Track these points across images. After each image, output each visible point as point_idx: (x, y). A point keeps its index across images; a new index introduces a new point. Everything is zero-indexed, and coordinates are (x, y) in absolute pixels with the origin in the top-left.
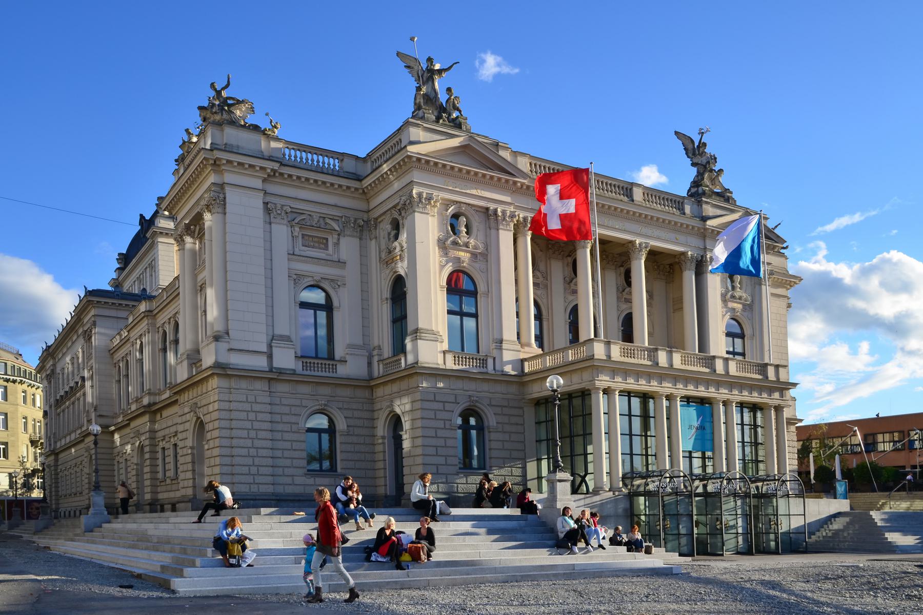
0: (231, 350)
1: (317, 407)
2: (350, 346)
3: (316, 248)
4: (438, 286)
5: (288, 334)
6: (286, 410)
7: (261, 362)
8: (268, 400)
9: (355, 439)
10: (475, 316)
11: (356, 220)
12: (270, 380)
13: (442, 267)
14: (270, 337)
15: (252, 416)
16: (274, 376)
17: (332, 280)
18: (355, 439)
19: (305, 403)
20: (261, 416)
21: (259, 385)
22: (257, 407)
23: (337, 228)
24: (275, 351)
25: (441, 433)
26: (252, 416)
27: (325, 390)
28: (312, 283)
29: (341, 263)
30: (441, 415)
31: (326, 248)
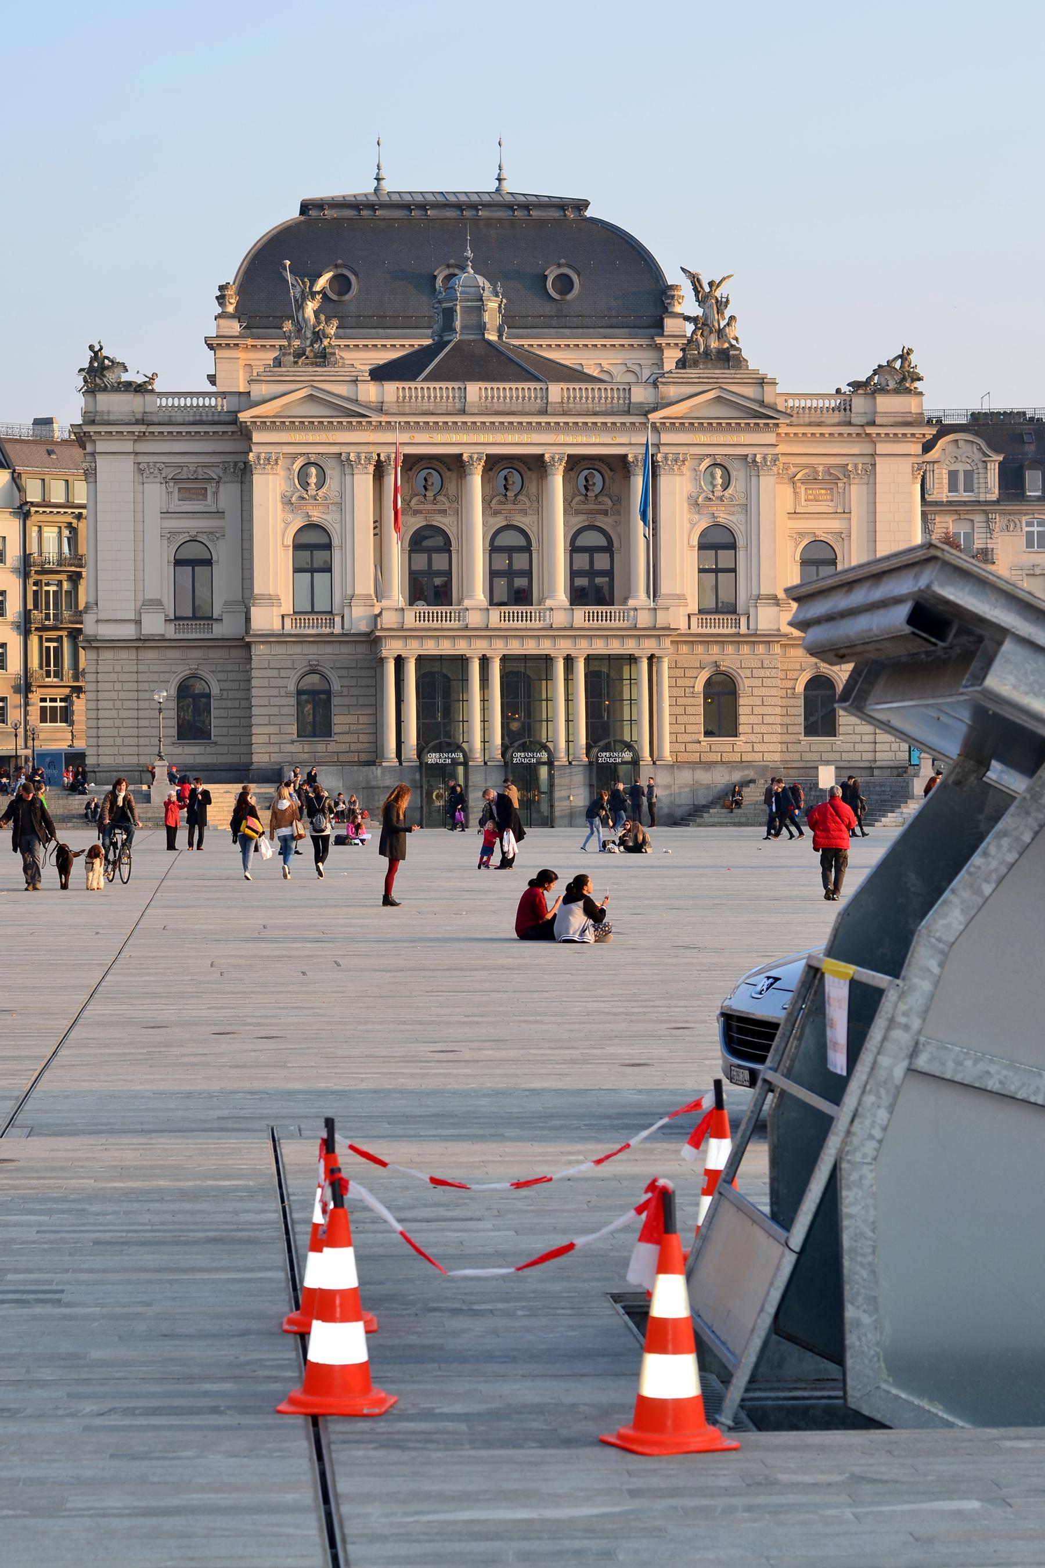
0: (97, 621)
1: (188, 672)
2: (227, 603)
3: (193, 500)
4: (279, 544)
5: (159, 597)
6: (155, 677)
7: (128, 631)
8: (135, 669)
9: (229, 704)
10: (329, 570)
11: (236, 463)
12: (137, 648)
13: (287, 524)
14: (140, 603)
15: (118, 686)
16: (142, 643)
17: (211, 533)
18: (229, 704)
19: (174, 668)
20: (126, 686)
21: (124, 654)
22: (123, 677)
23: (215, 477)
24: (145, 618)
25: (273, 701)
26: (118, 686)
27: (197, 654)
28: (188, 539)
29: (220, 513)
30: (280, 682)
31: (205, 497)
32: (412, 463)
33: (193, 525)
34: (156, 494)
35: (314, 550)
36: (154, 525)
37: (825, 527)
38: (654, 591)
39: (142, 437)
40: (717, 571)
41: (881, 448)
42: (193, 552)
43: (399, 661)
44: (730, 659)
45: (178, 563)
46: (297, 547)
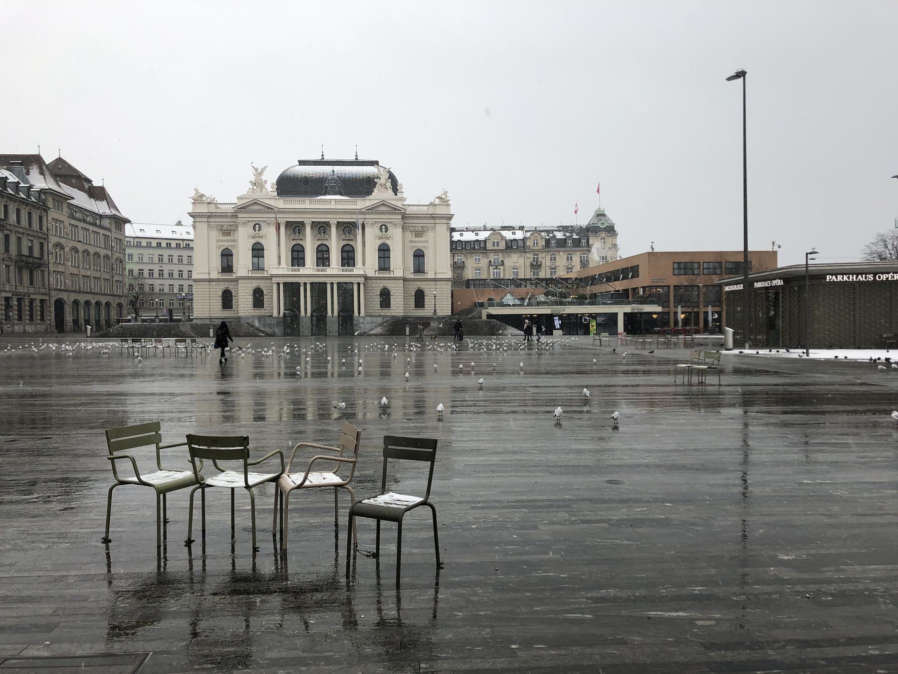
7: (206, 277)
16: (210, 280)
32: (288, 224)
33: (226, 245)
34: (215, 235)
35: (258, 251)
36: (214, 245)
37: (419, 246)
38: (364, 264)
39: (209, 217)
40: (384, 257)
41: (437, 221)
42: (226, 252)
43: (278, 284)
44: (389, 285)
45: (222, 255)
46: (253, 250)
